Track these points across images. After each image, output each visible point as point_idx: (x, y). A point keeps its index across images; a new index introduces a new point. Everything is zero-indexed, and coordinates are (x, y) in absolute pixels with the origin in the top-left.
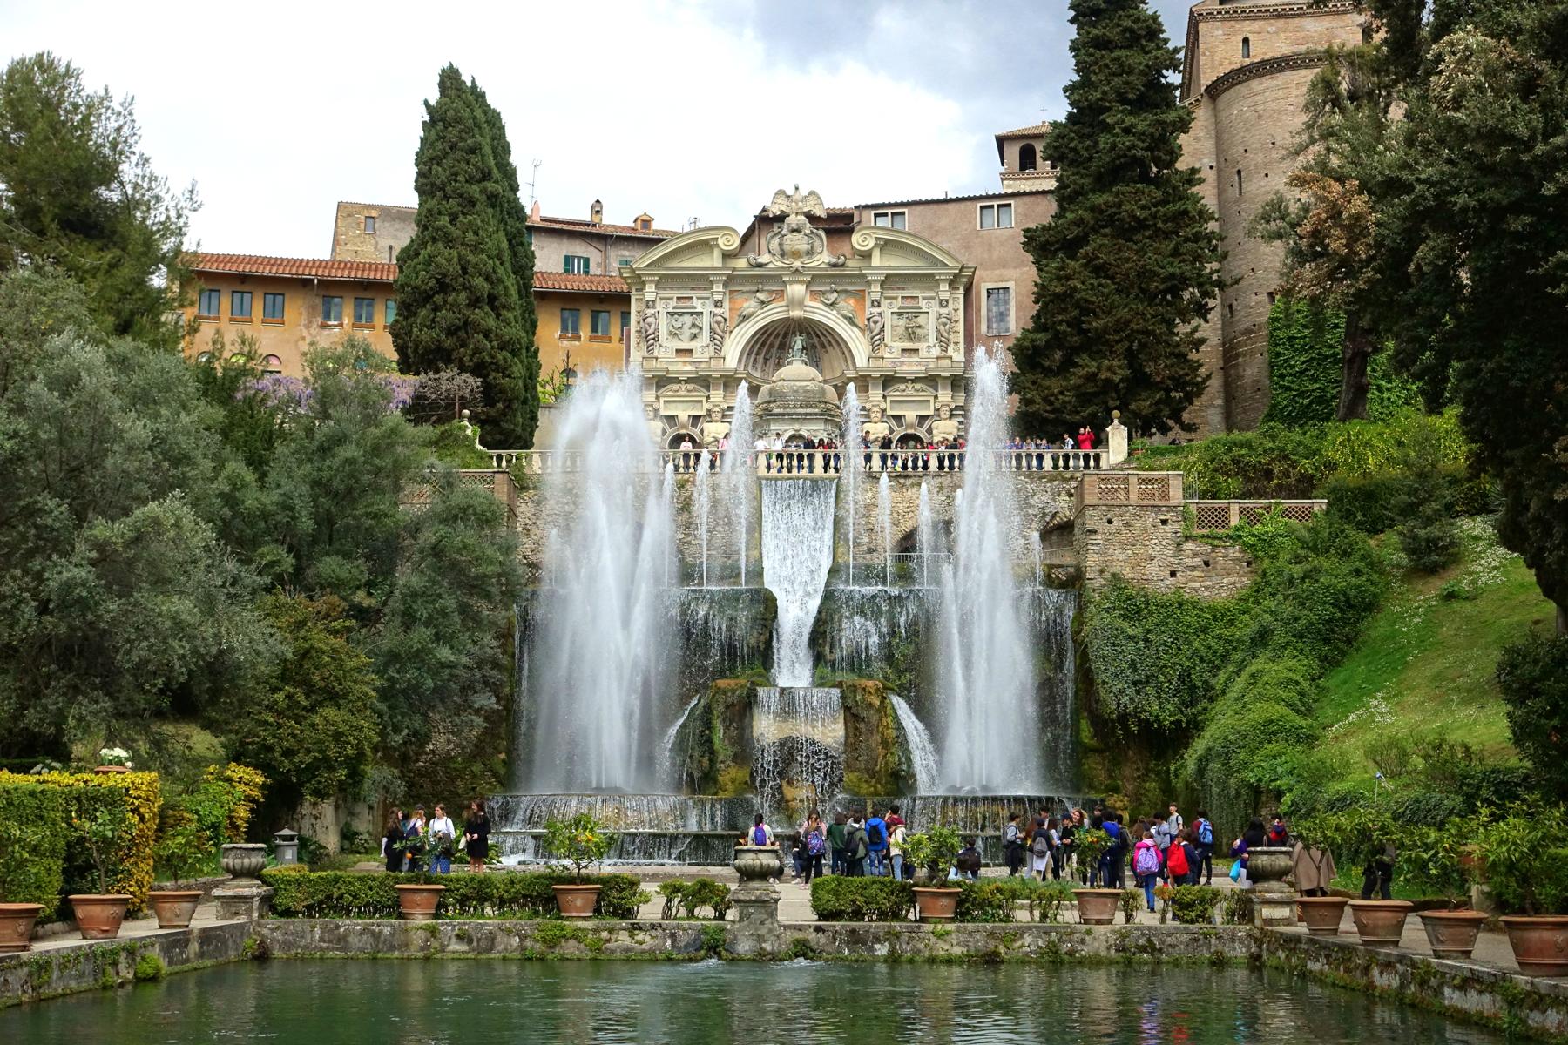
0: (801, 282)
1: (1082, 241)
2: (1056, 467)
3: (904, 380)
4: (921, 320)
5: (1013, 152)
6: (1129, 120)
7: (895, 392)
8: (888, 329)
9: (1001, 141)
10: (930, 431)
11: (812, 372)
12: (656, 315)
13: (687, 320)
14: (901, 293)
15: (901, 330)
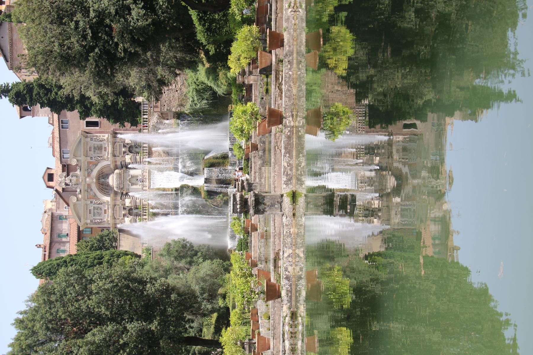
0: (85, 179)
1: (86, 107)
2: (146, 115)
3: (113, 151)
4: (96, 146)
5: (24, 113)
6: (53, 93)
7: (117, 154)
8: (99, 155)
9: (21, 117)
10: (128, 144)
11: (111, 177)
12: (95, 219)
13: (96, 211)
14: (89, 152)
15: (99, 152)
